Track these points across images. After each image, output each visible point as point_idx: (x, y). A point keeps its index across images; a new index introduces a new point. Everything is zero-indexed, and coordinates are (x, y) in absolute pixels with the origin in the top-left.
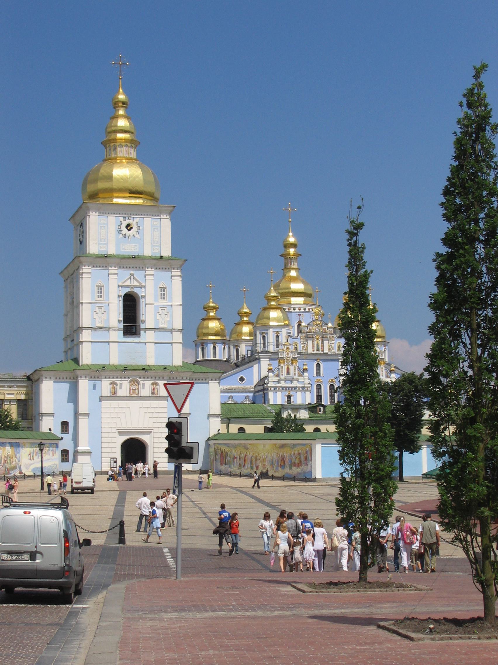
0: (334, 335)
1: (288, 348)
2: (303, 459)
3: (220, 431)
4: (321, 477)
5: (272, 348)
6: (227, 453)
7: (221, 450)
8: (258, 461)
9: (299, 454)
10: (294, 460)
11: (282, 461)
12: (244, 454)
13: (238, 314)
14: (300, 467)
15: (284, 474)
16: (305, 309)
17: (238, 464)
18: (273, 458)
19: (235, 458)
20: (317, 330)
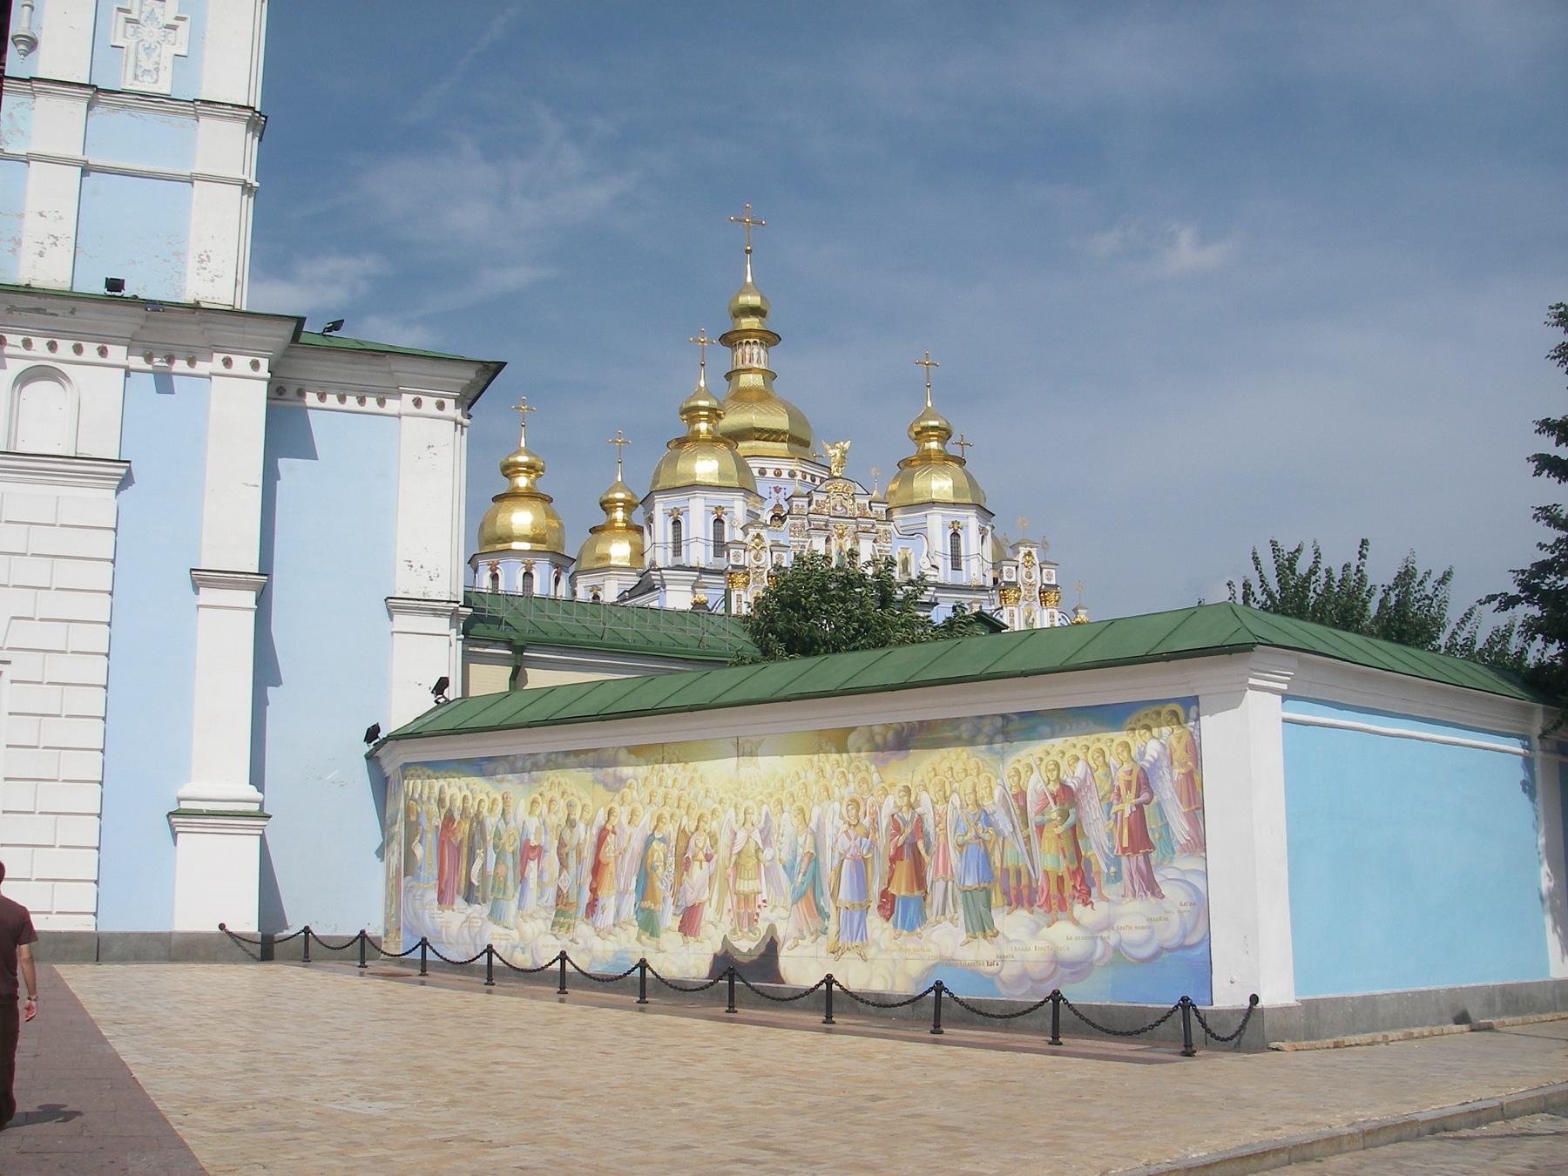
0: (891, 527)
1: (758, 534)
2: (1100, 835)
3: (453, 692)
4: (1291, 1000)
5: (700, 553)
6: (481, 823)
7: (441, 802)
8: (698, 873)
9: (1066, 796)
10: (1010, 855)
11: (903, 867)
12: (589, 824)
13: (601, 504)
14: (1078, 909)
15: (915, 967)
16: (792, 474)
17: (551, 893)
18: (817, 836)
19: (529, 852)
20: (839, 508)
